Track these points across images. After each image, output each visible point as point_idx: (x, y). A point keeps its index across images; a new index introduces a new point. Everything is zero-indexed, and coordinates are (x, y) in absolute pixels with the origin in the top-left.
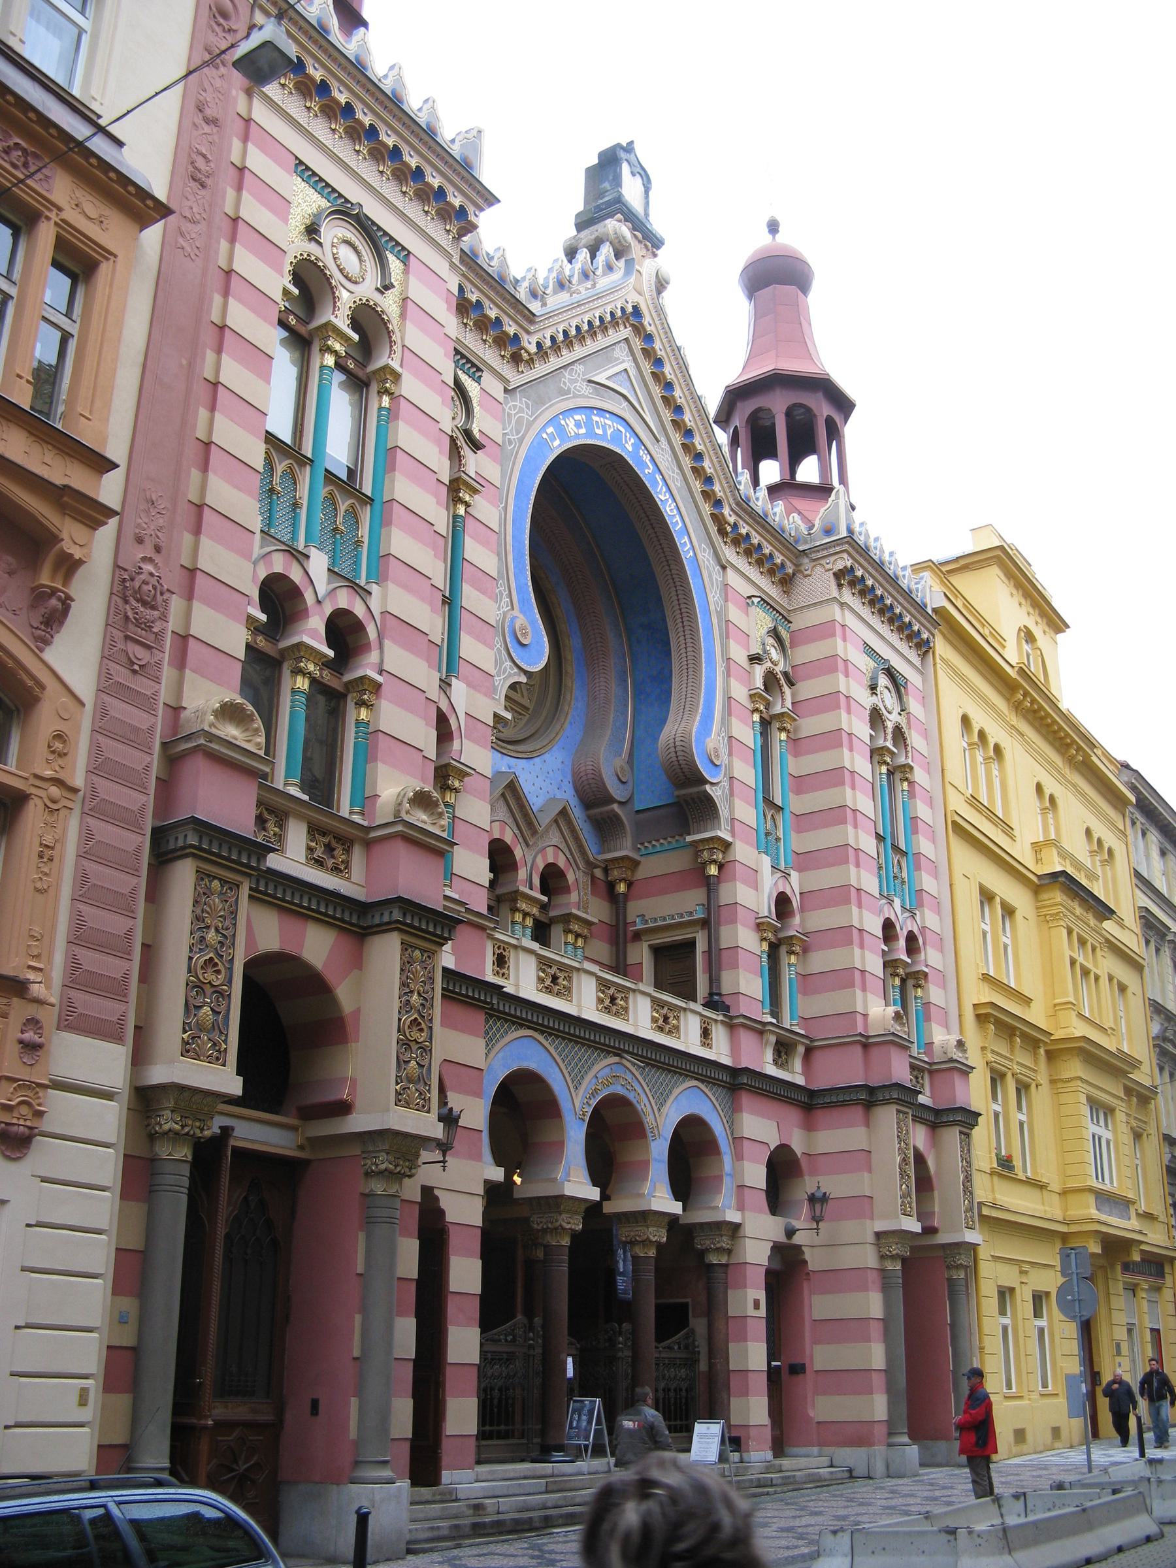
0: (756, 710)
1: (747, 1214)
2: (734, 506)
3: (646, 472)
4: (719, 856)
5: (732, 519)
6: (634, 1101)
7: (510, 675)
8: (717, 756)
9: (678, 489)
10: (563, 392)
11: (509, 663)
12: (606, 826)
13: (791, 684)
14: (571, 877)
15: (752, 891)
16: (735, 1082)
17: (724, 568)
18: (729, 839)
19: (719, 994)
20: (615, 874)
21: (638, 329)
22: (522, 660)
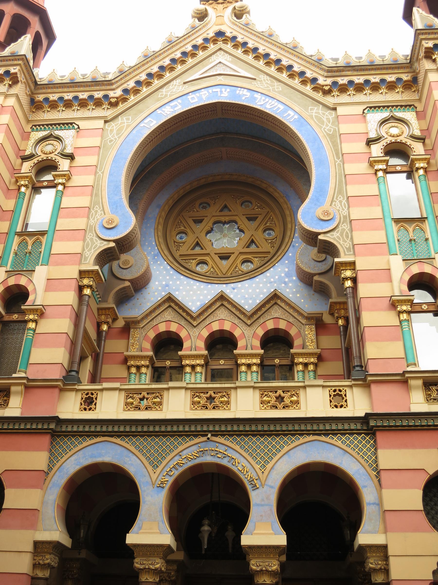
0: (377, 171)
1: (388, 533)
2: (326, 74)
3: (243, 98)
4: (348, 273)
5: (329, 81)
6: (229, 465)
7: (100, 247)
8: (328, 214)
9: (279, 92)
10: (158, 100)
11: (99, 241)
12: (322, 290)
13: (422, 139)
14: (293, 332)
15: (389, 284)
16: (369, 426)
17: (335, 109)
18: (350, 259)
19: (361, 366)
20: (336, 315)
21: (225, 41)
22: (110, 236)
